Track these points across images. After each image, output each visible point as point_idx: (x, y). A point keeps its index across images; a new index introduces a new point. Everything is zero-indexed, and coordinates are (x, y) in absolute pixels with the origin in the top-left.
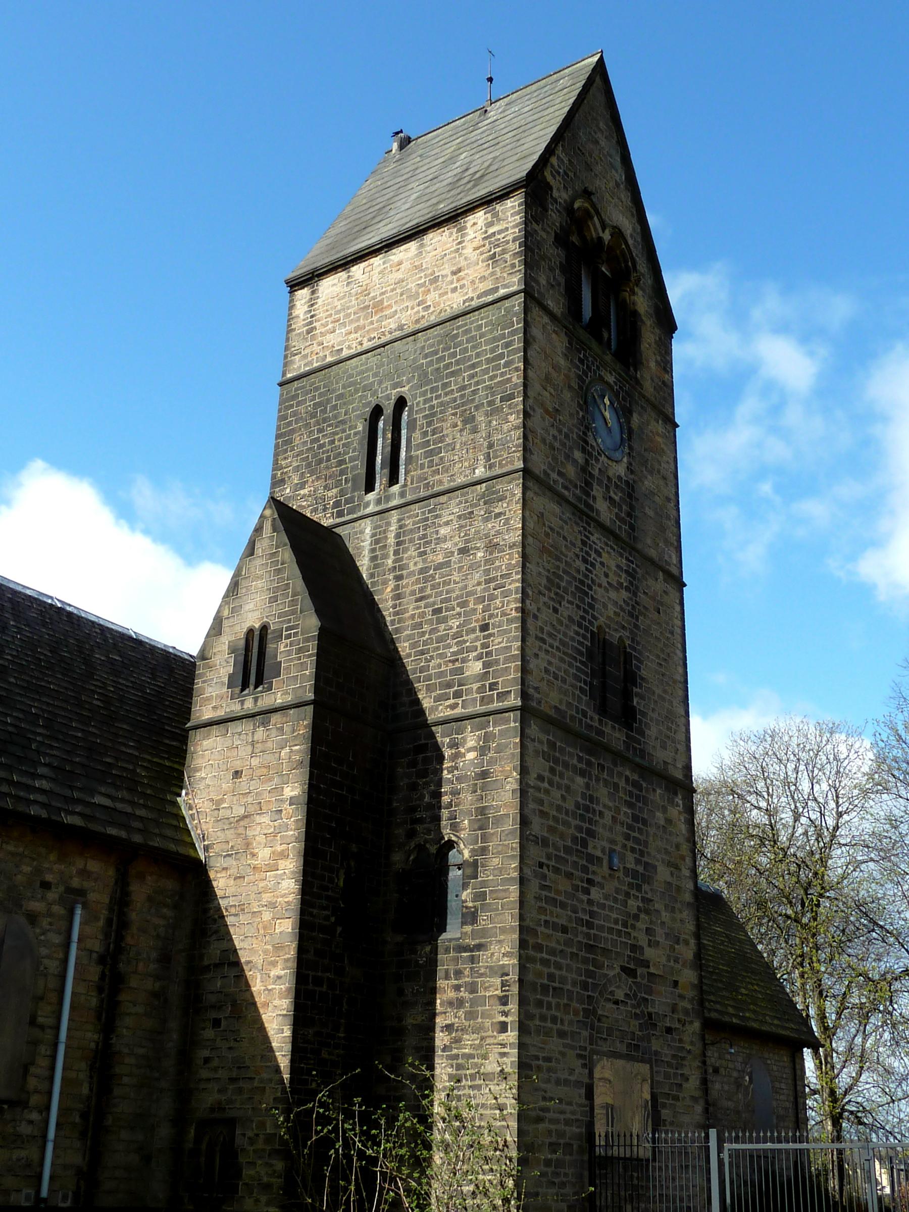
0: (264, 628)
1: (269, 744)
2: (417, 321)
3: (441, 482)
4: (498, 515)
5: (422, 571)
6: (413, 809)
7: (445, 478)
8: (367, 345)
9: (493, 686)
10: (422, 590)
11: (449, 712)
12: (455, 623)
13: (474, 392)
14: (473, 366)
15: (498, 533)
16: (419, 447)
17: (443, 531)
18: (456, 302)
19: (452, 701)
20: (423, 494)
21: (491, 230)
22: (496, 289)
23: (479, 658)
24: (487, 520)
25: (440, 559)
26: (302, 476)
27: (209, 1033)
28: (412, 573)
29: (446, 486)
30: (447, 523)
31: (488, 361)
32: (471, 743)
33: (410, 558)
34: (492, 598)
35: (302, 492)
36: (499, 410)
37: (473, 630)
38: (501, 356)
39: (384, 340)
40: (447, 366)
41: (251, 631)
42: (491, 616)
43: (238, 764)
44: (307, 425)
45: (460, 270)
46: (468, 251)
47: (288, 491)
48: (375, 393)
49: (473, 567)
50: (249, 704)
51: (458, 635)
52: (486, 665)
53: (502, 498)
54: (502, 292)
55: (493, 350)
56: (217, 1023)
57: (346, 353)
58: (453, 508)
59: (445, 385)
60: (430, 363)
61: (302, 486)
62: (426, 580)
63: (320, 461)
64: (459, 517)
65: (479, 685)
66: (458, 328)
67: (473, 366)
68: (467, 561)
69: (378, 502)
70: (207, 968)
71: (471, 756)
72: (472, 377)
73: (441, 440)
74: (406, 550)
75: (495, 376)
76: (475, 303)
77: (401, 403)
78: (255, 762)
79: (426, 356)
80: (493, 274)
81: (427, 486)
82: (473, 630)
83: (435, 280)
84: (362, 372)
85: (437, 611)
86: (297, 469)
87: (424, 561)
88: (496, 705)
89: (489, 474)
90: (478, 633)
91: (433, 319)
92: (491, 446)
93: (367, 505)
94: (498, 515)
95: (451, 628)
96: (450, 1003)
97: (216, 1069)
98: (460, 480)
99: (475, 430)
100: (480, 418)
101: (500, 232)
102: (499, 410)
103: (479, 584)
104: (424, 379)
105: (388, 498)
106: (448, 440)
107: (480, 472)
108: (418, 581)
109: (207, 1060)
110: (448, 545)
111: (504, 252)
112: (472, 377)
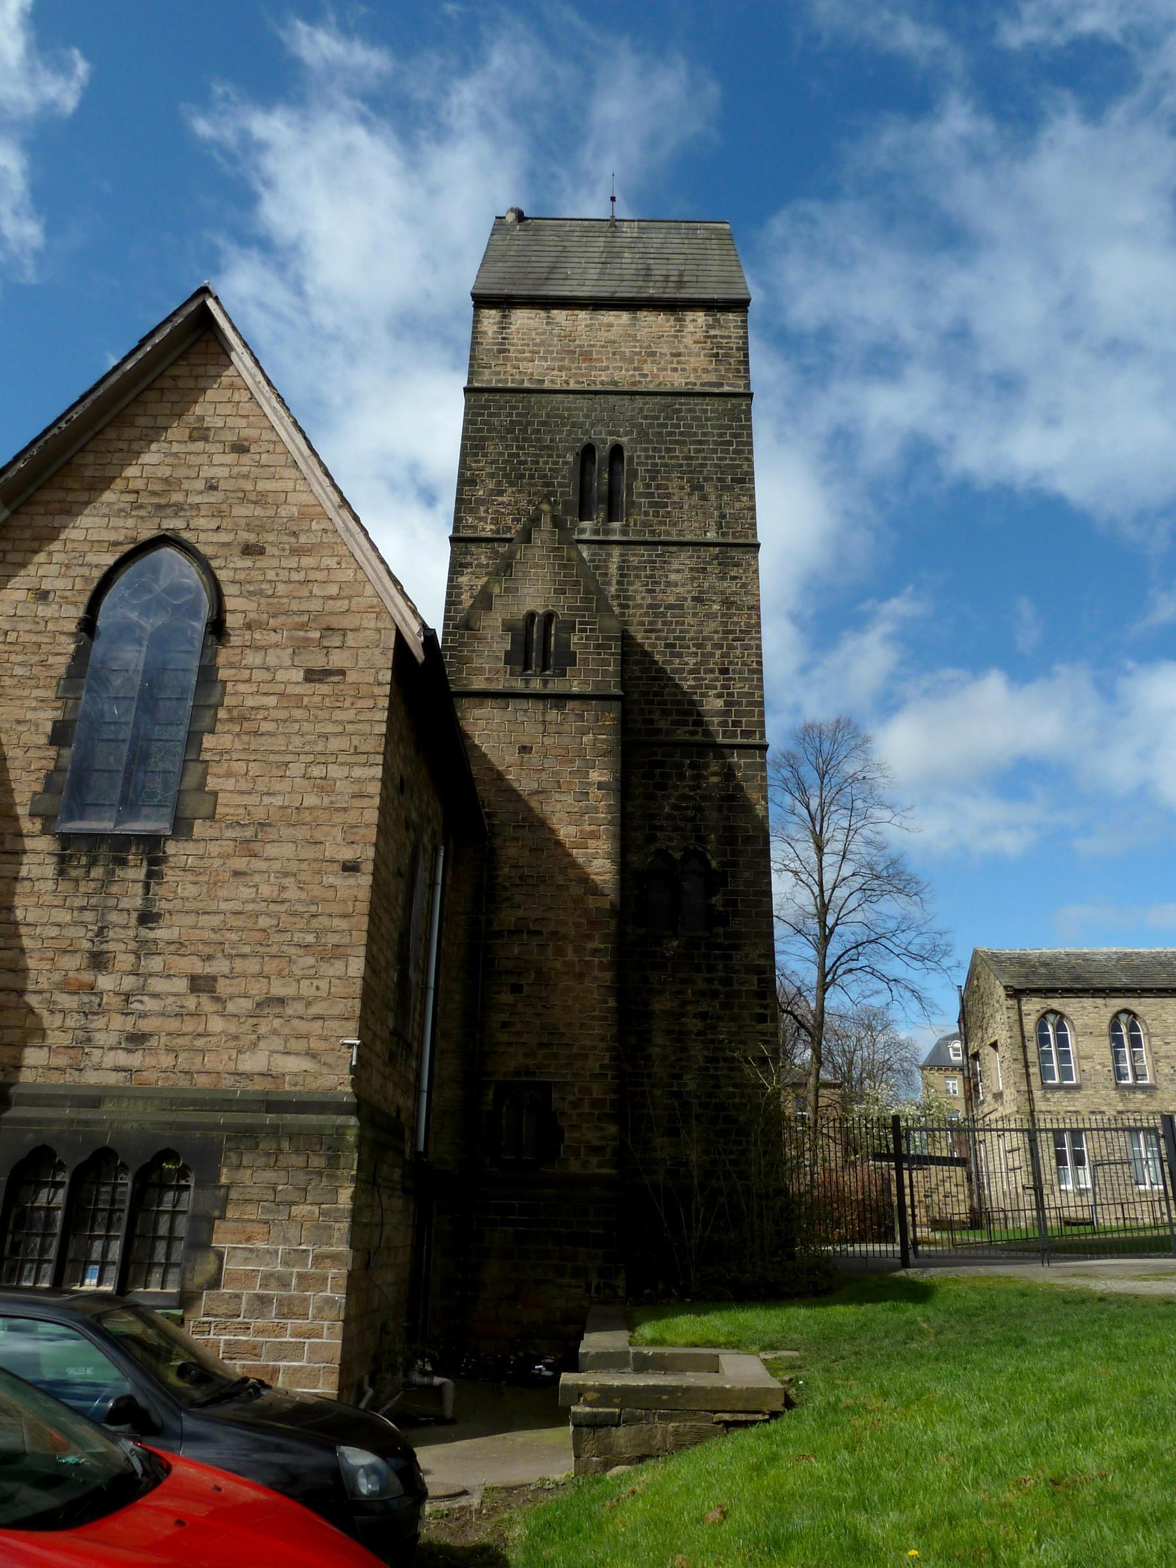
0: (549, 617)
1: (566, 727)
2: (634, 384)
3: (668, 533)
4: (734, 578)
5: (650, 606)
6: (653, 817)
7: (674, 531)
8: (573, 386)
9: (736, 724)
10: (651, 623)
11: (688, 737)
12: (692, 661)
13: (703, 465)
14: (700, 443)
15: (735, 593)
16: (640, 495)
17: (673, 577)
18: (678, 381)
19: (691, 728)
20: (648, 538)
21: (712, 332)
22: (721, 385)
23: (720, 696)
24: (723, 579)
25: (672, 600)
26: (499, 483)
27: (507, 998)
28: (640, 606)
29: (675, 538)
30: (678, 571)
31: (715, 442)
32: (714, 768)
33: (636, 591)
34: (730, 647)
35: (500, 499)
36: (732, 488)
37: (712, 671)
38: (730, 443)
39: (593, 388)
40: (670, 434)
41: (531, 616)
42: (730, 663)
43: (526, 740)
44: (502, 438)
45: (679, 355)
46: (688, 341)
47: (481, 493)
48: (586, 432)
49: (710, 616)
50: (536, 685)
51: (691, 672)
52: (726, 703)
53: (738, 565)
54: (726, 389)
55: (721, 435)
56: (516, 989)
57: (547, 385)
58: (682, 562)
59: (668, 450)
60: (651, 425)
61: (501, 493)
62: (656, 615)
63: (522, 476)
64: (692, 569)
65: (720, 719)
66: (681, 404)
67: (700, 443)
68: (700, 608)
69: (596, 532)
70: (500, 934)
71: (714, 779)
72: (698, 451)
73: (668, 496)
74: (631, 583)
75: (725, 459)
76: (698, 389)
77: (617, 450)
78: (547, 741)
79: (646, 417)
80: (716, 370)
81: (653, 532)
82: (712, 671)
83: (653, 354)
84: (569, 409)
85: (673, 646)
86: (492, 476)
87: (654, 598)
88: (739, 740)
89: (721, 540)
90: (717, 674)
91: (652, 387)
92: (722, 516)
93: (582, 531)
94: (734, 578)
95: (687, 664)
96: (703, 993)
97: (519, 1034)
98: (689, 537)
99: (704, 498)
100: (709, 488)
101: (722, 337)
102: (730, 488)
103: (716, 632)
104: (643, 436)
105: (607, 532)
106: (676, 499)
107: (711, 536)
108: (646, 614)
109: (505, 1025)
110: (680, 590)
111: (727, 355)
112: (698, 451)
